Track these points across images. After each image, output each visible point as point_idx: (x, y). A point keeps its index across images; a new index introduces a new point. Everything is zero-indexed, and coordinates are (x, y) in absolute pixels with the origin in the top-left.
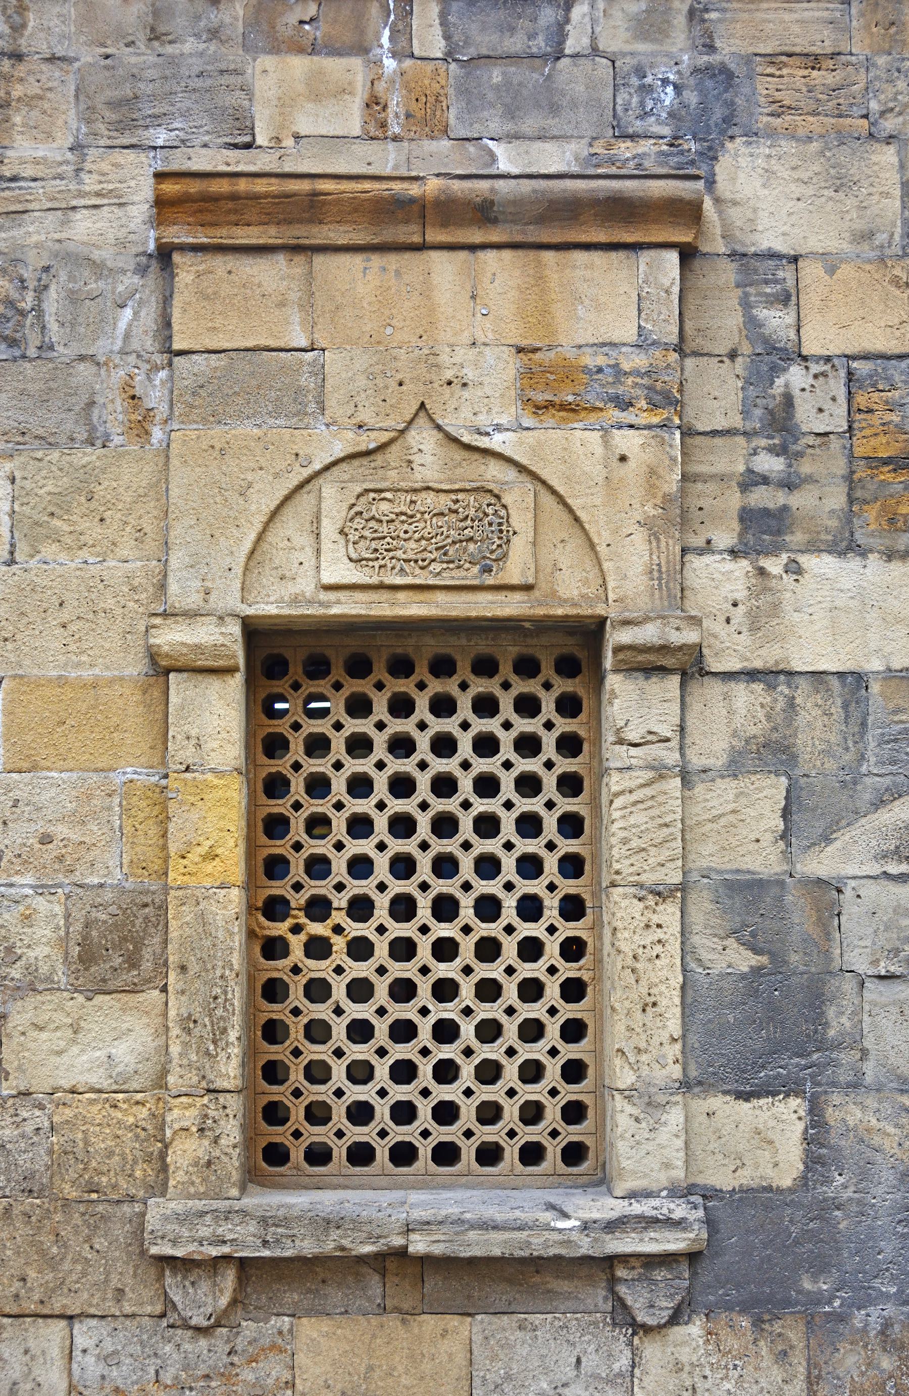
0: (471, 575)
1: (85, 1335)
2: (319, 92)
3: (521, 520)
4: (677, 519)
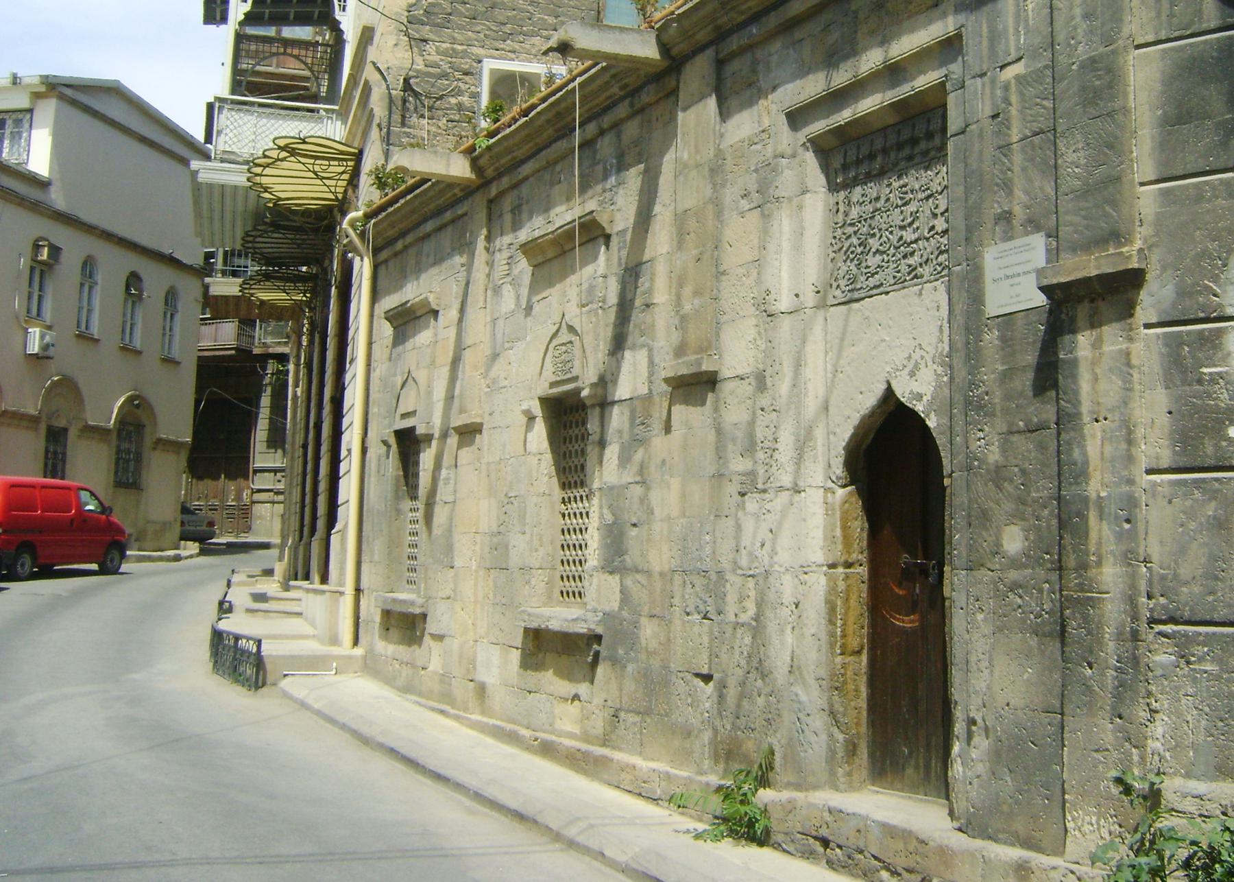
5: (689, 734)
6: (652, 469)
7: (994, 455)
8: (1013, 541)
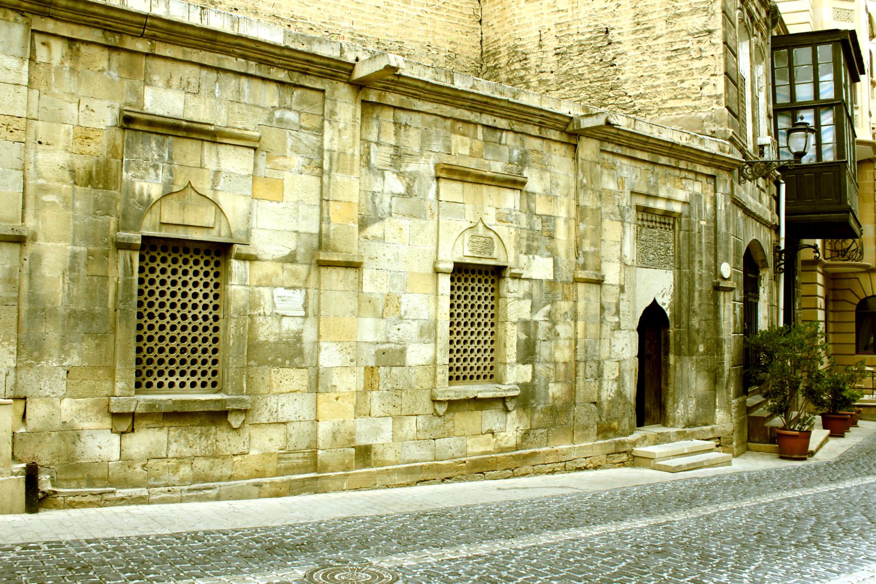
0: (487, 256)
1: (420, 418)
2: (464, 144)
3: (496, 245)
4: (518, 246)
5: (587, 428)
6: (558, 316)
7: (697, 326)
8: (701, 349)
